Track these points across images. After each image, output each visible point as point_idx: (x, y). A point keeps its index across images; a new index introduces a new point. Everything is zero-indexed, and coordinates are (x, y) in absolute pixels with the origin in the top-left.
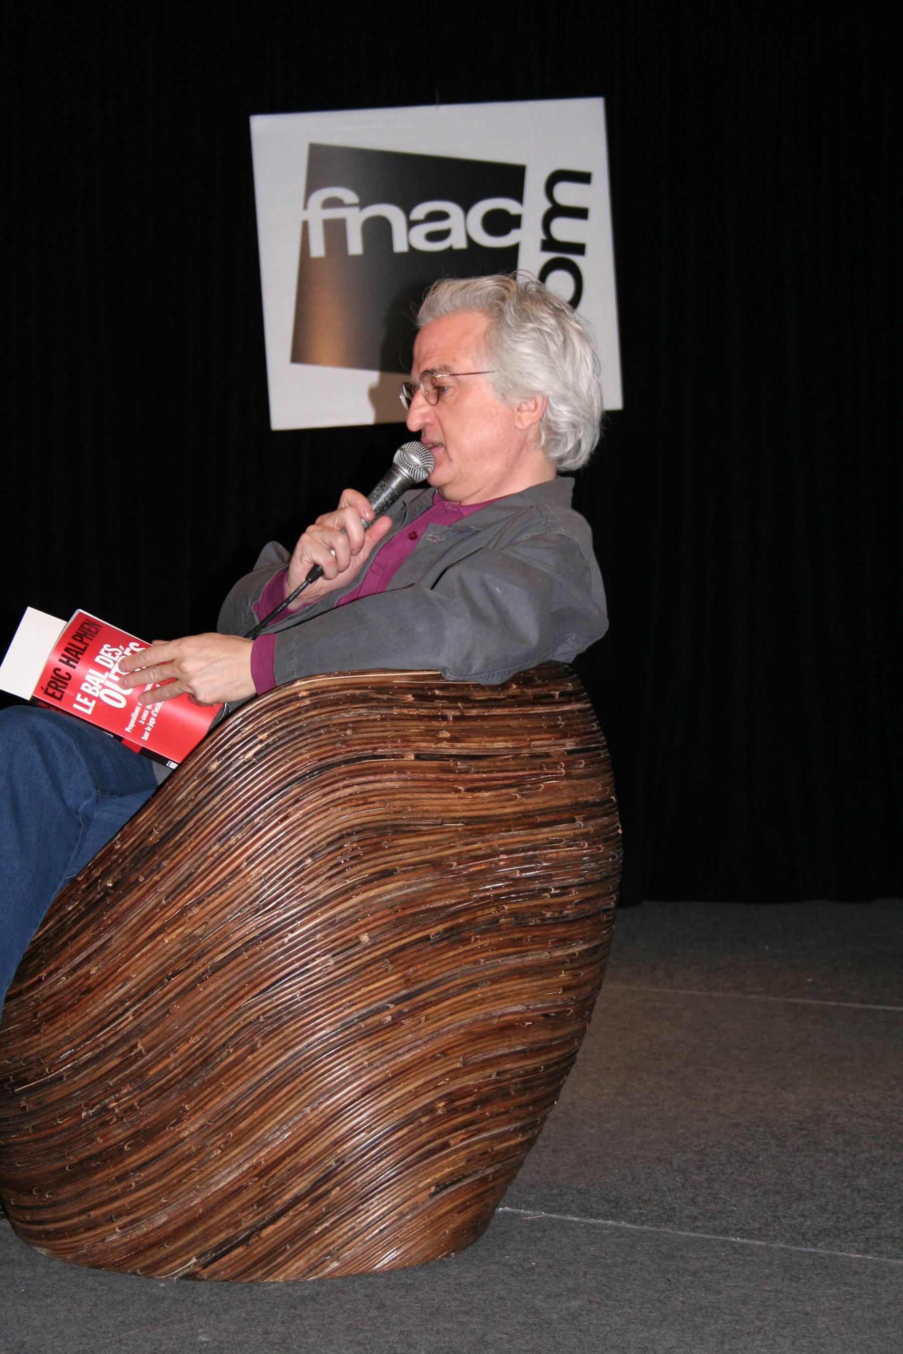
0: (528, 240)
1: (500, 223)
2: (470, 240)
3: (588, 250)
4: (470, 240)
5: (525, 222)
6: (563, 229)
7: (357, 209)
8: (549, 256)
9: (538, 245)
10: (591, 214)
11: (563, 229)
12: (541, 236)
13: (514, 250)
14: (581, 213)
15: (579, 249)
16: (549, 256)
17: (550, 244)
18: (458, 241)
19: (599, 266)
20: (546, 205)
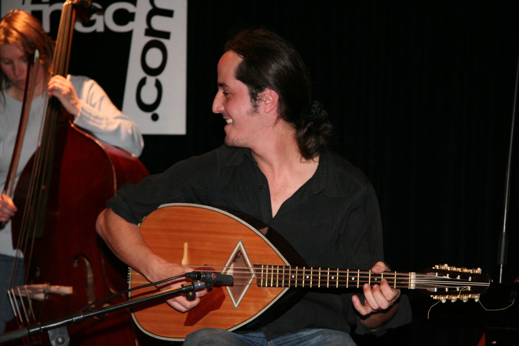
0: (137, 27)
1: (124, 17)
2: (106, 27)
3: (172, 36)
4: (106, 27)
5: (137, 17)
6: (159, 23)
7: (47, 6)
8: (149, 39)
9: (143, 32)
10: (175, 14)
11: (159, 23)
12: (145, 26)
13: (129, 35)
14: (169, 13)
15: (166, 35)
16: (149, 39)
17: (150, 31)
18: (99, 27)
19: (178, 47)
20: (149, 8)
